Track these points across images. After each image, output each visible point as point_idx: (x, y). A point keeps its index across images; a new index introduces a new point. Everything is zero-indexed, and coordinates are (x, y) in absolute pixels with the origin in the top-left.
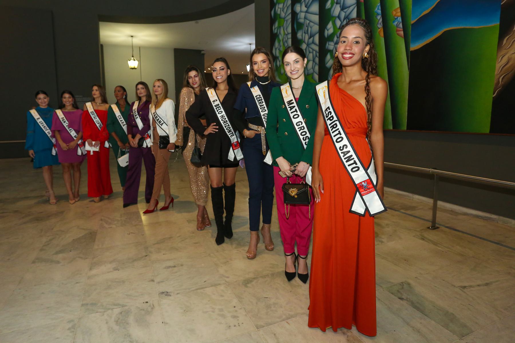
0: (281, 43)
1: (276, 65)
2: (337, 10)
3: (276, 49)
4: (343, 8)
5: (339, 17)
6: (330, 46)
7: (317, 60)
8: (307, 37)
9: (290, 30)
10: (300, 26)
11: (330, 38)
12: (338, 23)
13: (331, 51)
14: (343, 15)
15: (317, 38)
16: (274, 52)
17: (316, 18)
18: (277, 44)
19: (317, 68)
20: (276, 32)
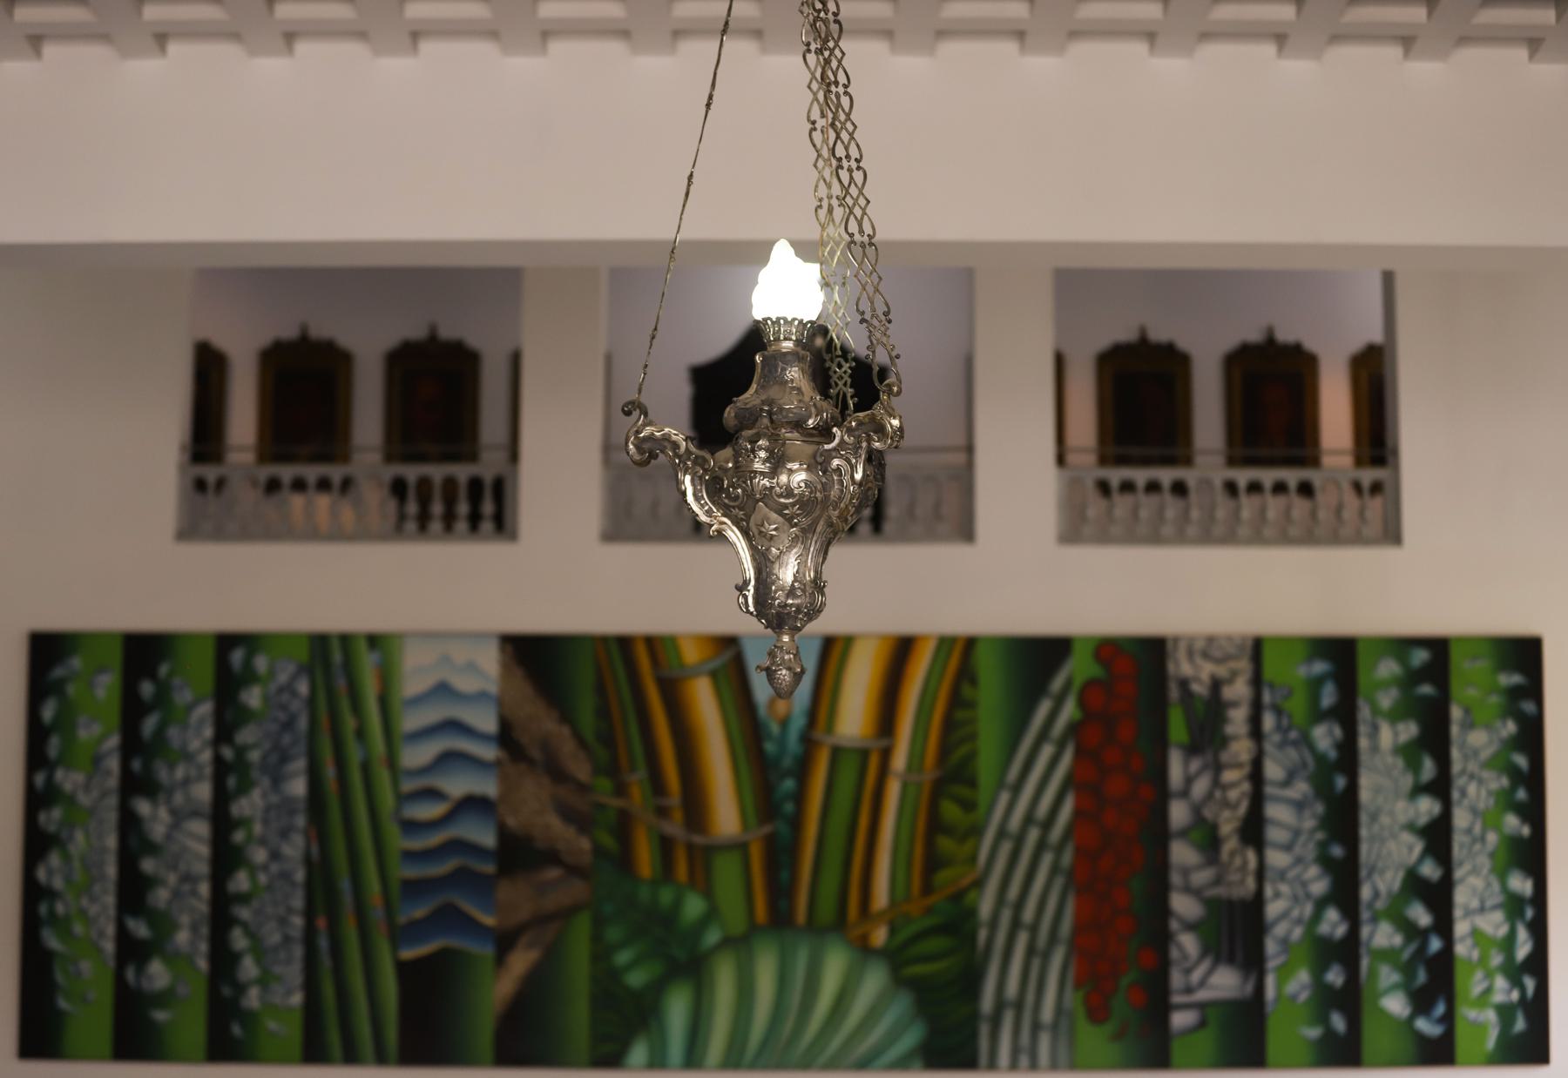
0: (77, 865)
1: (52, 913)
2: (260, 855)
3: (50, 873)
4: (275, 855)
5: (265, 868)
6: (244, 913)
7: (205, 930)
8: (172, 879)
9: (112, 841)
10: (152, 848)
11: (244, 899)
12: (263, 878)
13: (245, 926)
14: (274, 868)
15: (204, 889)
16: (41, 874)
17: (204, 850)
18: (54, 859)
19: (204, 947)
20: (52, 828)
